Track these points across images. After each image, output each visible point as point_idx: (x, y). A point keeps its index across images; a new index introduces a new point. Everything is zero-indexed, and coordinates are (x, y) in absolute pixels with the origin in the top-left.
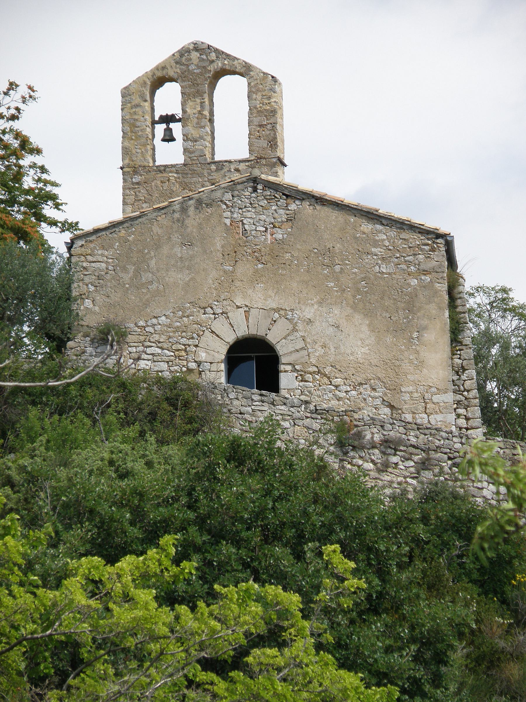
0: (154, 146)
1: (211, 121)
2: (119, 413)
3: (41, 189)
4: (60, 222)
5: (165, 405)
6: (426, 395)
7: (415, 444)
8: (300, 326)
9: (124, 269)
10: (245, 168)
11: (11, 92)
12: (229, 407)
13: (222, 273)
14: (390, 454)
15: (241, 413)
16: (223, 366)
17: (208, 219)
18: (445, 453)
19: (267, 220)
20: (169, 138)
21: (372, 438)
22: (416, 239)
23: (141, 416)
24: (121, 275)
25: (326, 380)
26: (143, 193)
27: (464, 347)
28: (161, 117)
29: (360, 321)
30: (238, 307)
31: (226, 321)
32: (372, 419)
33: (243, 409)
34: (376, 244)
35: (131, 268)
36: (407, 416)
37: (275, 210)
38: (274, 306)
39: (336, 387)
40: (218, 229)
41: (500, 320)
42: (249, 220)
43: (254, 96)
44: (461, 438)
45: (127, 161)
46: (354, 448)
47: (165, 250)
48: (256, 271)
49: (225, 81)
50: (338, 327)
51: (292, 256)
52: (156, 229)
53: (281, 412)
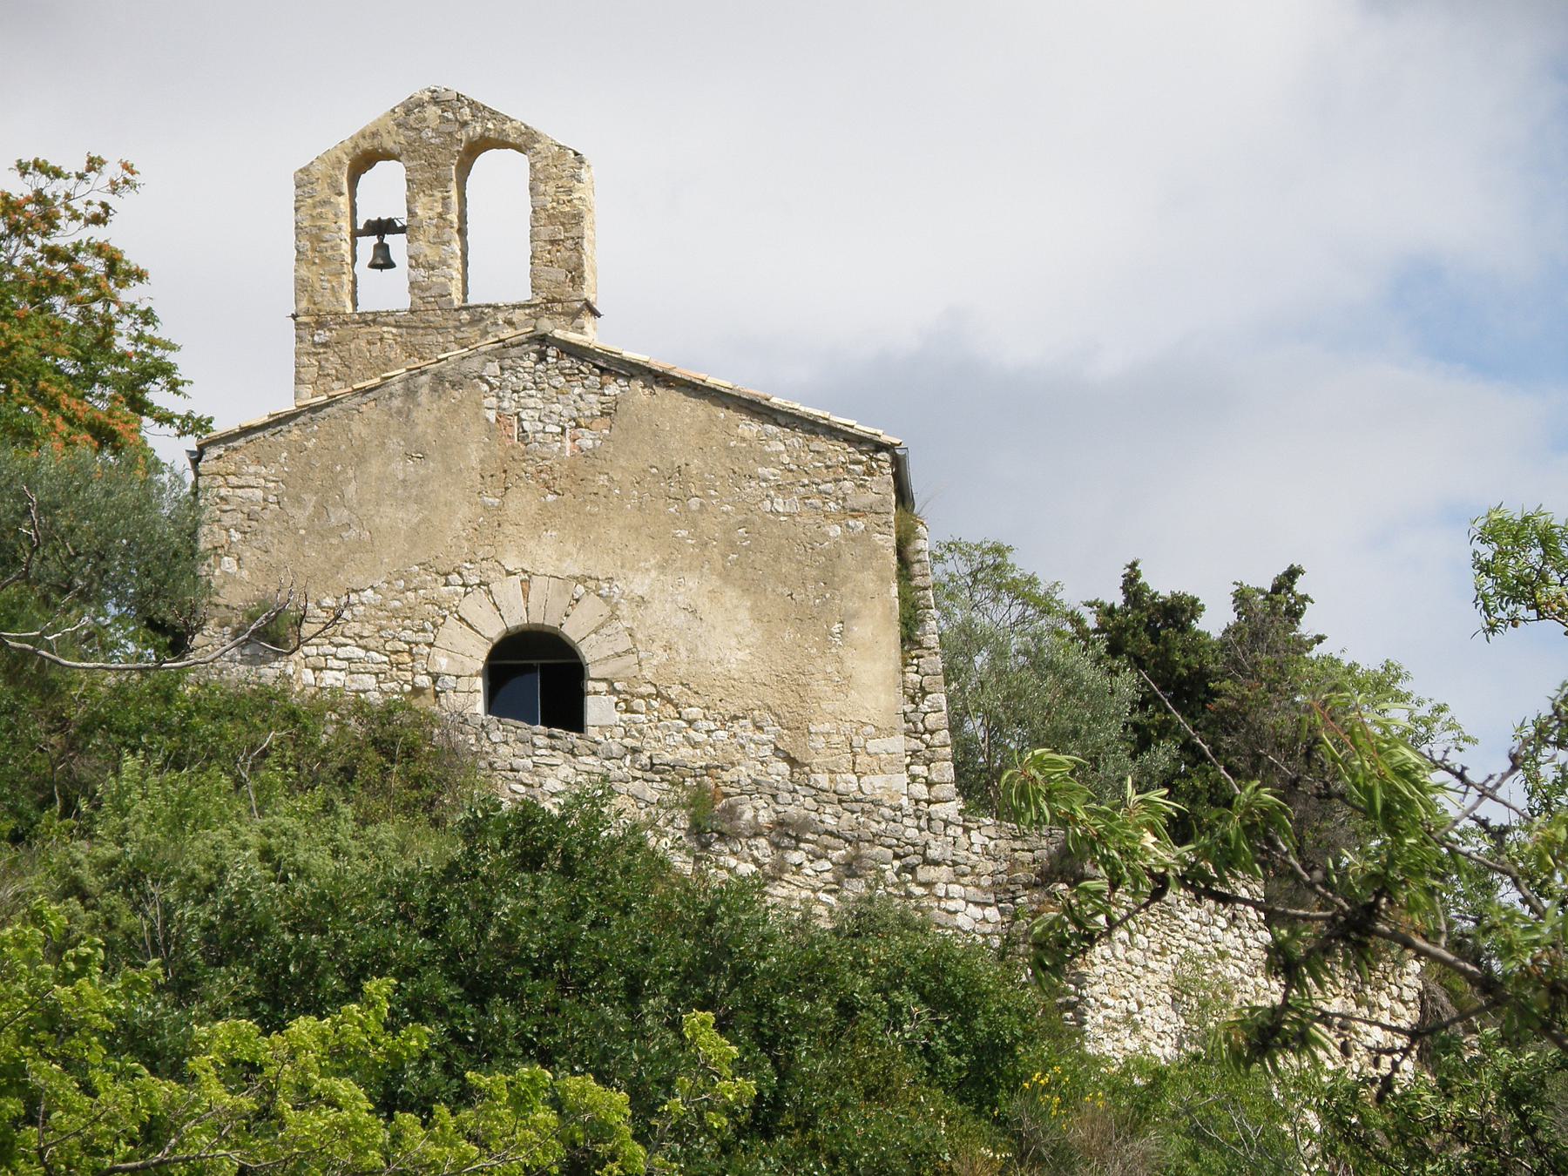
0: (355, 276)
1: (462, 232)
2: (285, 767)
3: (143, 355)
4: (179, 417)
5: (371, 753)
6: (855, 738)
7: (834, 829)
8: (624, 610)
9: (298, 501)
10: (523, 318)
11: (92, 175)
12: (490, 758)
13: (479, 510)
14: (787, 848)
15: (512, 770)
16: (479, 683)
17: (454, 411)
18: (889, 847)
19: (565, 413)
20: (383, 261)
21: (755, 817)
22: (839, 452)
23: (325, 774)
24: (292, 511)
25: (670, 710)
26: (333, 362)
27: (925, 652)
28: (369, 224)
29: (735, 601)
30: (509, 573)
31: (486, 600)
32: (756, 782)
33: (517, 762)
34: (765, 460)
35: (311, 499)
36: (819, 777)
37: (580, 395)
38: (578, 572)
39: (690, 723)
40: (474, 429)
41: (990, 605)
42: (531, 412)
43: (542, 187)
44: (919, 818)
45: (304, 304)
46: (722, 836)
47: (375, 467)
48: (544, 507)
49: (487, 162)
50: (694, 612)
51: (611, 480)
52: (357, 427)
53: (588, 768)
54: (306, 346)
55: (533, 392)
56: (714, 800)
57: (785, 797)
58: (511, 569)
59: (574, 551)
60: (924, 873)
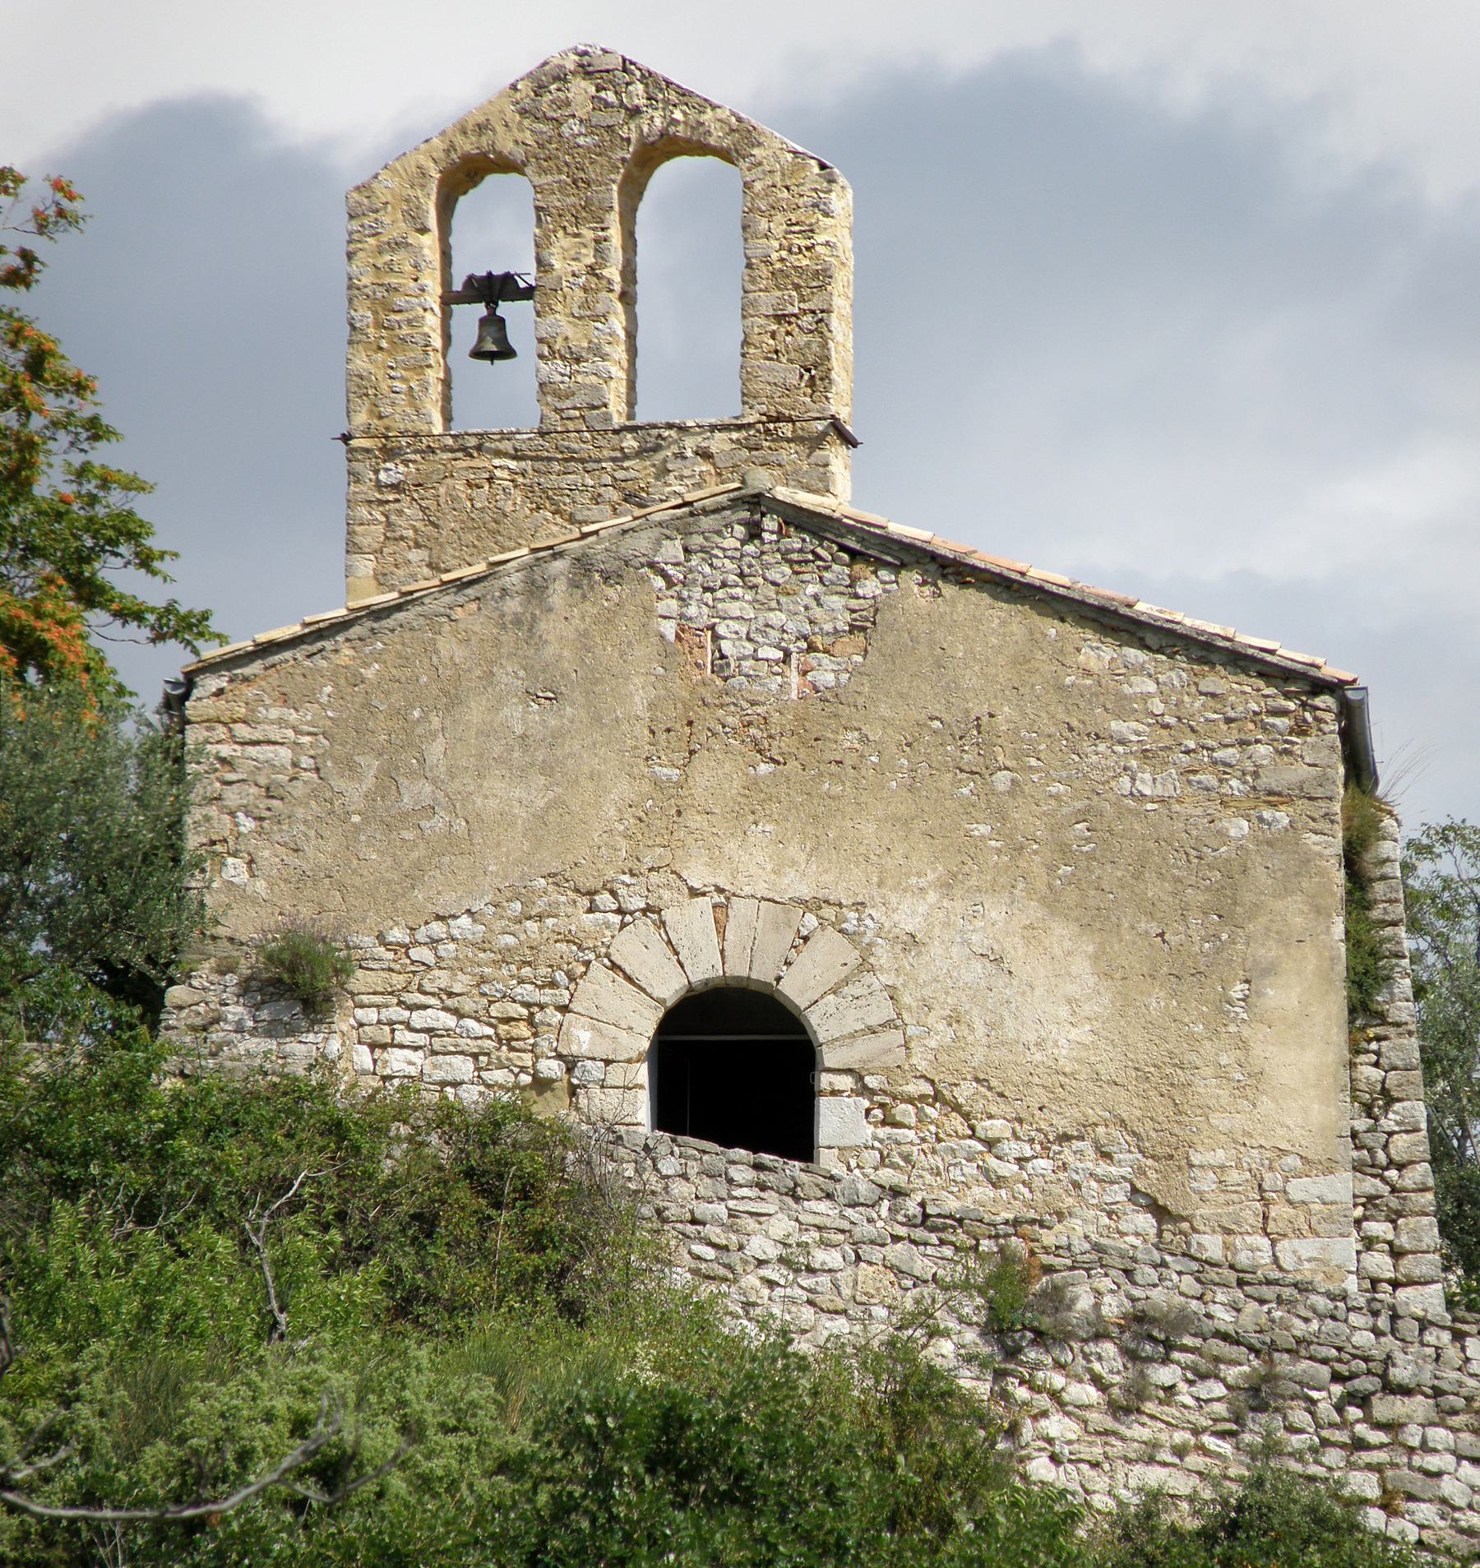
3: (93, 500)
4: (152, 610)
5: (462, 1192)
6: (1267, 1176)
7: (1230, 1329)
8: (883, 955)
9: (350, 767)
13: (647, 787)
14: (1149, 1360)
16: (642, 1074)
17: (608, 619)
19: (790, 626)
21: (1097, 1306)
24: (339, 784)
25: (957, 1122)
27: (1391, 1031)
29: (1067, 944)
30: (694, 893)
31: (655, 938)
32: (1097, 1248)
33: (702, 1209)
34: (1123, 707)
35: (371, 765)
36: (1205, 1239)
37: (816, 597)
38: (806, 892)
39: (990, 1144)
40: (640, 651)
43: (763, 224)
44: (1375, 1314)
45: (361, 418)
47: (475, 712)
48: (752, 785)
50: (998, 961)
51: (864, 739)
52: (448, 646)
53: (818, 1220)
54: (367, 490)
55: (739, 591)
56: (1026, 1280)
57: (1147, 1274)
58: (696, 884)
59: (802, 857)
60: (1384, 1408)
